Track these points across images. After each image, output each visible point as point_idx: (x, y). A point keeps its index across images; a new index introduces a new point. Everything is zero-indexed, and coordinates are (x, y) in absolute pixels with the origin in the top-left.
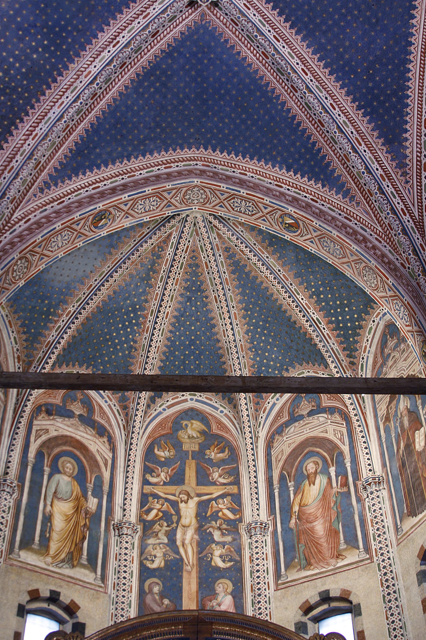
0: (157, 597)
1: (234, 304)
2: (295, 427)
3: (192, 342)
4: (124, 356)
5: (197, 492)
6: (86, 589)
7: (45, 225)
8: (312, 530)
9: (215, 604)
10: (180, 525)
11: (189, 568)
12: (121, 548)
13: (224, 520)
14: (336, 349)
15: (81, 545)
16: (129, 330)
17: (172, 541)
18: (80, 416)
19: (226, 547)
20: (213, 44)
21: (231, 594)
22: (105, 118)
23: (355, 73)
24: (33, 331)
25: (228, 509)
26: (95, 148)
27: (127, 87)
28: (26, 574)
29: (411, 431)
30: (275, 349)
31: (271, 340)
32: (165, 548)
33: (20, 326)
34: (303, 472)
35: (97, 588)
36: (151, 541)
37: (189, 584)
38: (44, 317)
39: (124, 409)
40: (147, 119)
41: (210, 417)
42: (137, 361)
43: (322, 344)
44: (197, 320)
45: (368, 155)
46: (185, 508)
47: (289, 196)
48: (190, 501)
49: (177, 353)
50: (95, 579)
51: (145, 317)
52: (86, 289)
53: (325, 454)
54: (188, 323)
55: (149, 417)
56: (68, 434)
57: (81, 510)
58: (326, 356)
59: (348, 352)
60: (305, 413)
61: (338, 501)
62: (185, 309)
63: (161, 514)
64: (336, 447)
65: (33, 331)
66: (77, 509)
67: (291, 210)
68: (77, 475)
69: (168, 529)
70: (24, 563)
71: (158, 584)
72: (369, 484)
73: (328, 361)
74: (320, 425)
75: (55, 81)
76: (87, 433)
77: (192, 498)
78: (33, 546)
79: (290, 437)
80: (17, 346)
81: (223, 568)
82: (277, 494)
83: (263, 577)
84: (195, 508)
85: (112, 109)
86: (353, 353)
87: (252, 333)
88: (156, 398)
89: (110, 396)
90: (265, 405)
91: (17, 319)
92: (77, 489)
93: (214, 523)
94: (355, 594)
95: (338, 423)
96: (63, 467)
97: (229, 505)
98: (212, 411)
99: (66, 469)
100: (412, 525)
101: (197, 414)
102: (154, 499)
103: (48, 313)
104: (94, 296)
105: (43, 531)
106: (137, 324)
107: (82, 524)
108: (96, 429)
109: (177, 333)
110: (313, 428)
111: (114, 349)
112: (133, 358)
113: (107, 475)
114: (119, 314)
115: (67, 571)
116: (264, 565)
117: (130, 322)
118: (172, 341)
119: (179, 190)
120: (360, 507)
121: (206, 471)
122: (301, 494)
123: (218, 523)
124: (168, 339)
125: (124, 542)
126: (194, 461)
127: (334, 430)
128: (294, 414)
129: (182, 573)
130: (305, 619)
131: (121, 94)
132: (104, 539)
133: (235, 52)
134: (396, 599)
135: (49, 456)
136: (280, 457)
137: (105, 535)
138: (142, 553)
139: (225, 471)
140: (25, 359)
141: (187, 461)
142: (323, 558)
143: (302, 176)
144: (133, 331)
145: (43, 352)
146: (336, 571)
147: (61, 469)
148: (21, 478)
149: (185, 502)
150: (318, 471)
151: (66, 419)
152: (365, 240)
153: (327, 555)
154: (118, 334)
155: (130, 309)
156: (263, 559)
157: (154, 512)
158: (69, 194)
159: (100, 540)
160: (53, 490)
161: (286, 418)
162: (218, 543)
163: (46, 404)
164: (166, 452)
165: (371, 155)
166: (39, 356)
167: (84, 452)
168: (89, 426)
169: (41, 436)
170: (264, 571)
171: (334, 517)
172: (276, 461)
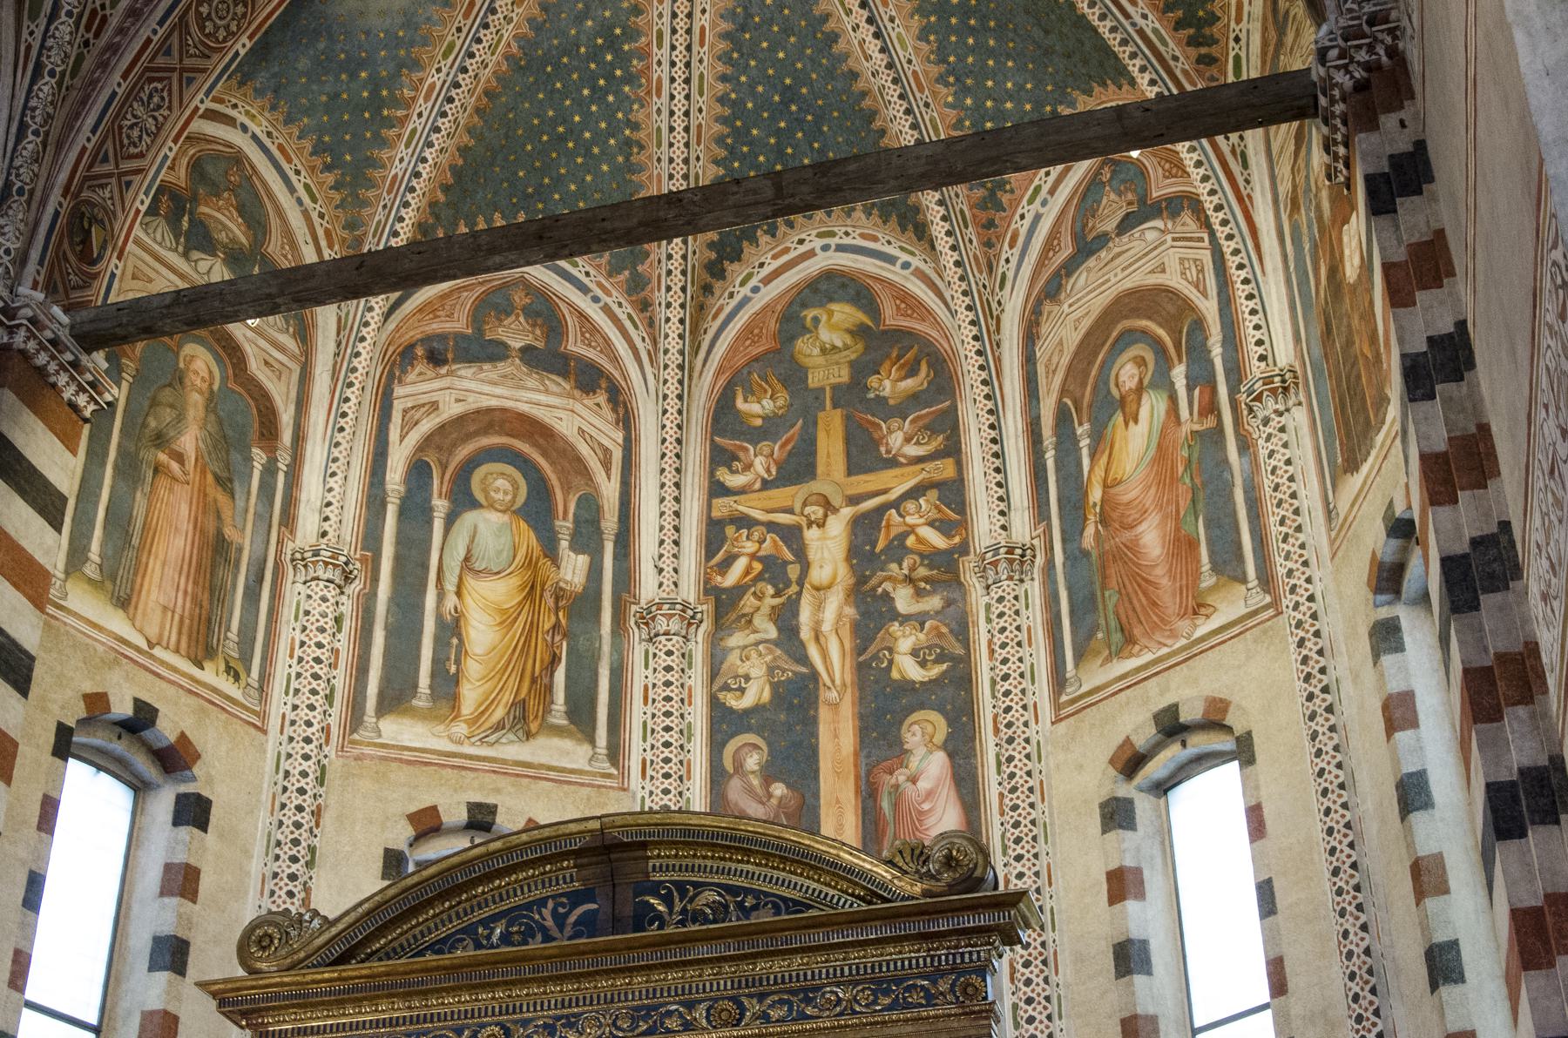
0: (755, 782)
2: (1089, 270)
3: (789, 95)
4: (616, 170)
5: (849, 492)
6: (566, 787)
8: (1134, 547)
9: (902, 778)
10: (807, 585)
11: (835, 694)
12: (655, 670)
13: (922, 556)
14: (1155, 31)
15: (546, 680)
16: (611, 98)
18: (526, 351)
19: (927, 625)
21: (944, 747)
24: (348, 158)
25: (931, 524)
28: (400, 774)
29: (1336, 229)
30: (1010, 64)
31: (992, 43)
32: (771, 652)
33: (312, 154)
34: (1109, 392)
35: (600, 781)
36: (736, 640)
37: (836, 736)
38: (367, 115)
39: (642, 311)
41: (877, 287)
42: (650, 177)
43: (1108, 23)
44: (787, 30)
46: (819, 539)
48: (831, 519)
49: (755, 132)
50: (590, 760)
51: (644, 55)
52: (460, 17)
53: (1161, 332)
54: (765, 45)
55: (715, 317)
56: (494, 403)
57: (543, 590)
58: (1124, 53)
59: (1192, 31)
60: (1110, 226)
61: (1196, 455)
62: (745, 8)
63: (758, 567)
64: (1187, 306)
65: (348, 158)
66: (531, 591)
68: (525, 504)
69: (777, 601)
70: (393, 747)
71: (756, 747)
72: (1259, 398)
73: (1130, 68)
74: (1146, 255)
76: (547, 391)
77: (836, 511)
78: (415, 702)
79: (1079, 300)
80: (318, 207)
81: (921, 683)
82: (1050, 464)
83: (1017, 691)
84: (844, 535)
86: (1207, 31)
87: (936, 33)
88: (726, 263)
89: (604, 282)
90: (1013, 226)
91: (299, 138)
92: (528, 539)
93: (894, 566)
94: (1239, 707)
95: (1190, 239)
96: (485, 491)
97: (934, 514)
98: (881, 268)
99: (492, 494)
100: (1353, 497)
101: (844, 286)
102: (738, 529)
103: (376, 104)
104: (482, 32)
105: (438, 663)
106: (630, 79)
107: (547, 626)
108: (572, 377)
109: (743, 79)
110: (1130, 265)
111: (584, 157)
112: (640, 169)
113: (610, 490)
114: (575, 63)
115: (512, 750)
116: (1020, 660)
117: (610, 77)
118: (734, 104)
120: (1246, 467)
121: (870, 434)
122: (1107, 453)
123: (905, 565)
125: (662, 654)
126: (839, 410)
127: (1182, 260)
128: (1084, 237)
129: (816, 710)
130: (1125, 790)
132: (611, 655)
134: (1330, 709)
135: (444, 467)
136: (1055, 360)
137: (613, 644)
138: (714, 674)
139: (921, 423)
140: (345, 234)
141: (821, 415)
142: (1162, 620)
144: (624, 101)
145: (385, 206)
146: (1194, 651)
147: (479, 496)
148: (371, 539)
149: (819, 526)
150: (1146, 382)
151: (486, 366)
153: (1170, 611)
154: (587, 115)
155: (600, 41)
156: (1019, 644)
157: (740, 565)
159: (599, 658)
160: (462, 553)
161: (1067, 251)
162: (905, 619)
163: (427, 339)
164: (764, 402)
166: (376, 219)
167: (541, 441)
168: (551, 372)
169: (416, 424)
170: (1022, 675)
171: (1184, 503)
172: (1047, 373)
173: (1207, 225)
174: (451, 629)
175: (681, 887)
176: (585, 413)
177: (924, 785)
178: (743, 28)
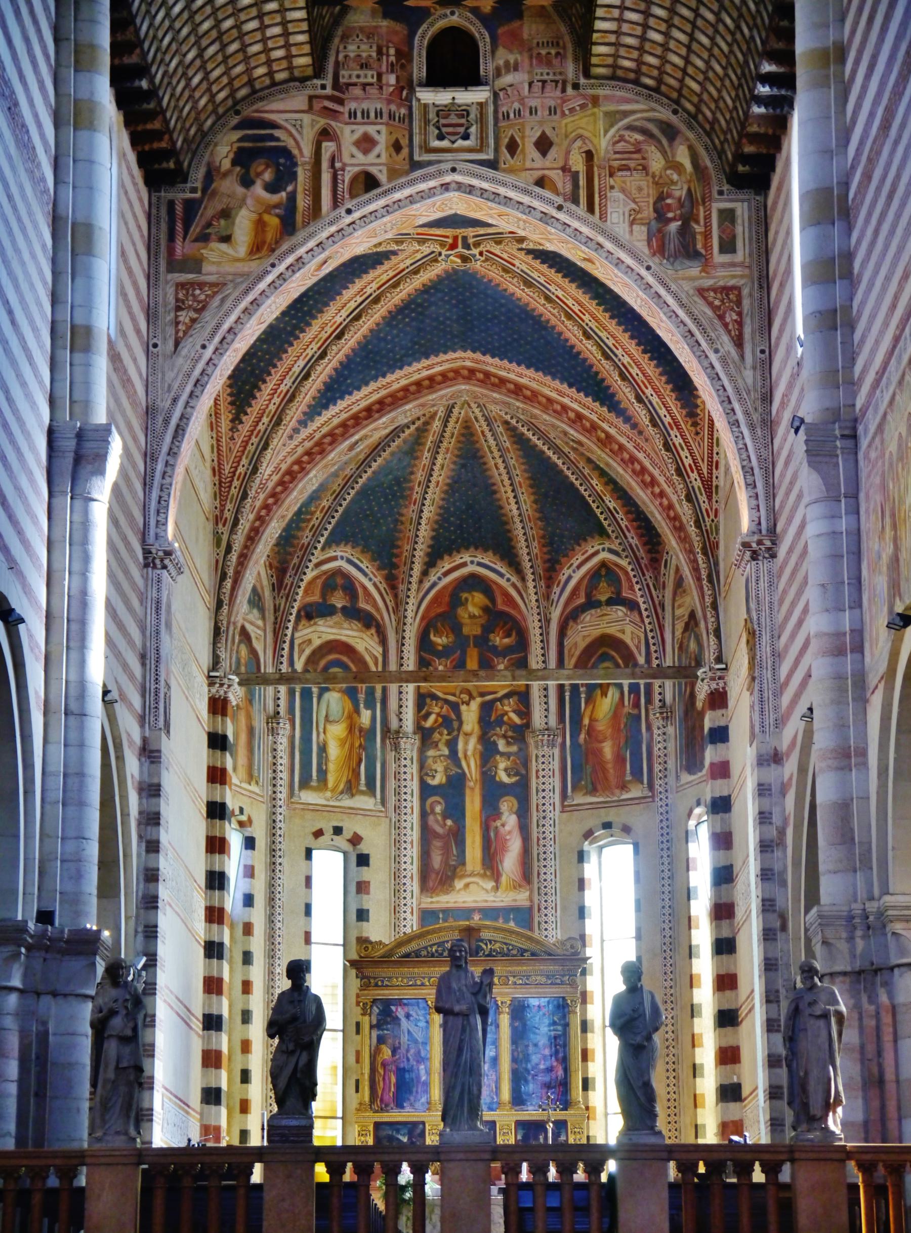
0: (439, 818)
1: (518, 472)
7: (299, 475)
8: (600, 751)
17: (454, 753)
21: (516, 813)
25: (514, 711)
26: (346, 379)
27: (378, 324)
28: (309, 815)
36: (431, 753)
41: (494, 587)
44: (475, 485)
45: (655, 400)
47: (573, 410)
51: (412, 489)
56: (332, 637)
60: (603, 598)
66: (351, 729)
67: (572, 432)
75: (298, 338)
76: (352, 630)
77: (474, 698)
82: (567, 698)
92: (349, 705)
97: (515, 707)
105: (319, 765)
107: (357, 744)
112: (400, 531)
115: (347, 802)
117: (394, 496)
119: (442, 397)
124: (440, 508)
138: (422, 766)
146: (621, 803)
152: (654, 482)
157: (432, 718)
160: (323, 713)
161: (582, 600)
162: (502, 754)
173: (643, 621)
174: (323, 749)
175: (490, 941)
176: (367, 639)
177: (507, 828)
178: (456, 482)
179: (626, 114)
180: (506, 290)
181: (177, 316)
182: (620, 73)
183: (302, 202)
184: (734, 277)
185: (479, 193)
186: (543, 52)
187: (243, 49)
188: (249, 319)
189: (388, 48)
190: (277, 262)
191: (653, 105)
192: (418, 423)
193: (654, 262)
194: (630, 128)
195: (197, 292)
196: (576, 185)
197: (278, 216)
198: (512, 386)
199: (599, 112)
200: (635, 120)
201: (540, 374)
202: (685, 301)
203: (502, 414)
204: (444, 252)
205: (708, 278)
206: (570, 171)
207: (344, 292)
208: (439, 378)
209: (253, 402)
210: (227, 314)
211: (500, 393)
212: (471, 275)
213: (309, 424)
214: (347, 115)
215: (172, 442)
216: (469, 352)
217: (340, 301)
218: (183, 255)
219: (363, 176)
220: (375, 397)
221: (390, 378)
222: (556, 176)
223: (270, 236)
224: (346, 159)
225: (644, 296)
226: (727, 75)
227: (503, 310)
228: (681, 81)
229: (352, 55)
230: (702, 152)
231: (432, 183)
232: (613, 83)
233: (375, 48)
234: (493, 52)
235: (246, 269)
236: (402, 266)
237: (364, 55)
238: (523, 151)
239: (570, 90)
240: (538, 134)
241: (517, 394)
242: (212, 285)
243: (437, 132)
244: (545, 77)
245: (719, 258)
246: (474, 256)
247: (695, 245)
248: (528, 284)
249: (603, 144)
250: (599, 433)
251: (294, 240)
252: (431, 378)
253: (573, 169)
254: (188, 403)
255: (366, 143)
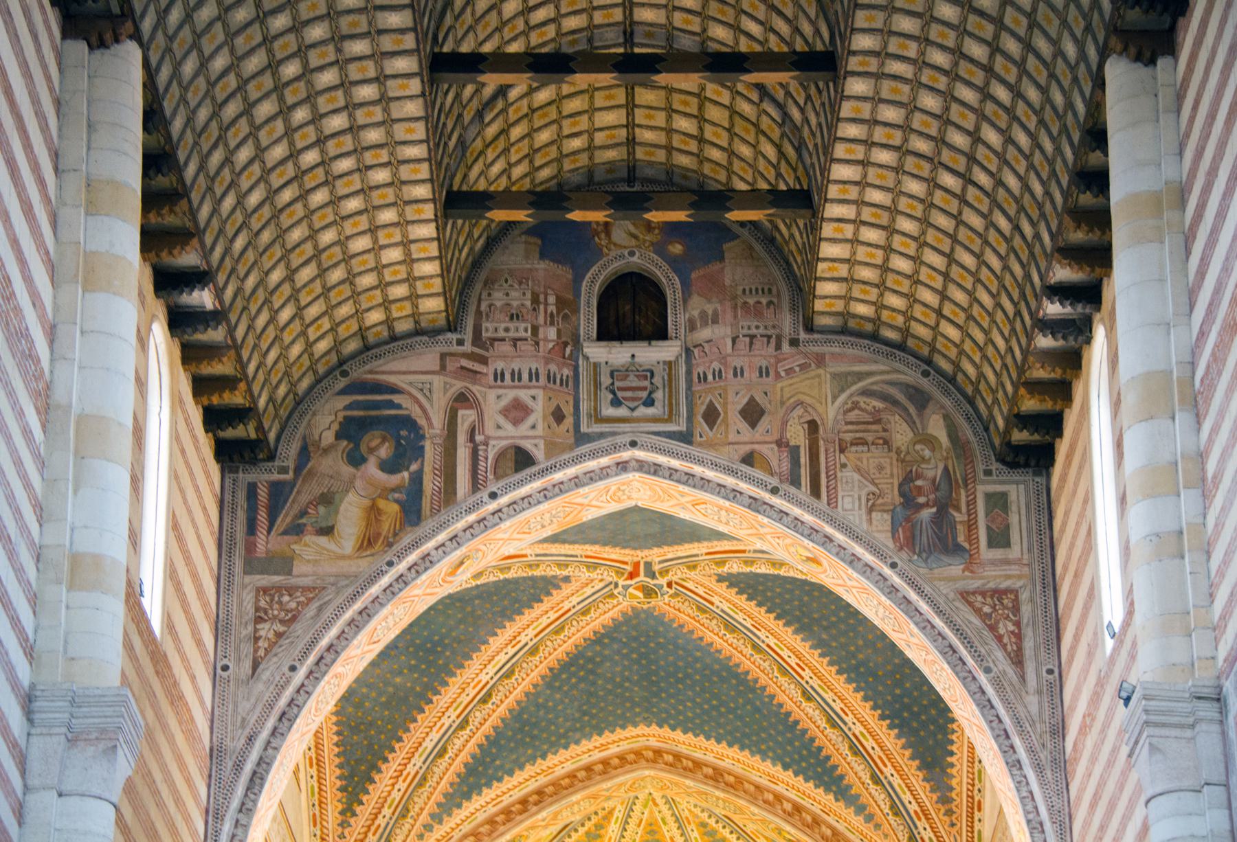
20: (661, 629)
22: (506, 725)
23: (875, 676)
26: (493, 761)
27: (535, 686)
40: (569, 711)
47: (788, 800)
67: (788, 828)
75: (431, 702)
85: (515, 713)
119: (620, 785)
131: (527, 694)
133: (695, 636)
143: (806, 780)
158: (458, 825)
165: (900, 781)
179: (861, 376)
180: (701, 639)
181: (256, 630)
182: (852, 324)
183: (430, 484)
184: (1008, 577)
185: (667, 474)
186: (751, 301)
187: (350, 279)
188: (356, 634)
189: (546, 295)
190: (395, 559)
191: (897, 365)
192: (588, 825)
193: (901, 558)
194: (865, 393)
195: (286, 598)
196: (795, 462)
197: (397, 501)
198: (710, 771)
199: (825, 374)
200: (872, 384)
201: (747, 752)
202: (943, 606)
203: (697, 811)
204: (621, 583)
205: (973, 578)
206: (787, 445)
207: (491, 640)
208: (616, 761)
209: (371, 788)
210: (327, 627)
211: (694, 780)
212: (655, 618)
213: (446, 818)
214: (491, 377)
215: (246, 795)
216: (654, 726)
217: (486, 652)
218: (267, 552)
219: (512, 451)
220: (532, 786)
221: (552, 760)
222: (769, 451)
223: (386, 527)
224: (490, 429)
225: (888, 602)
226: (998, 305)
227: (698, 666)
228: (935, 328)
229: (498, 304)
230: (961, 421)
231: (604, 461)
232: (843, 338)
233: (529, 295)
234: (685, 301)
235: (354, 569)
236: (567, 605)
237: (515, 304)
238: (725, 421)
239: (786, 347)
240: (745, 400)
241: (717, 781)
242: (306, 589)
243: (611, 396)
244: (754, 331)
245: (986, 553)
246: (661, 587)
247: (955, 538)
248: (730, 627)
249: (830, 413)
250: (824, 828)
251: (420, 531)
252: (605, 762)
253: (792, 443)
254: (269, 742)
255: (517, 411)
